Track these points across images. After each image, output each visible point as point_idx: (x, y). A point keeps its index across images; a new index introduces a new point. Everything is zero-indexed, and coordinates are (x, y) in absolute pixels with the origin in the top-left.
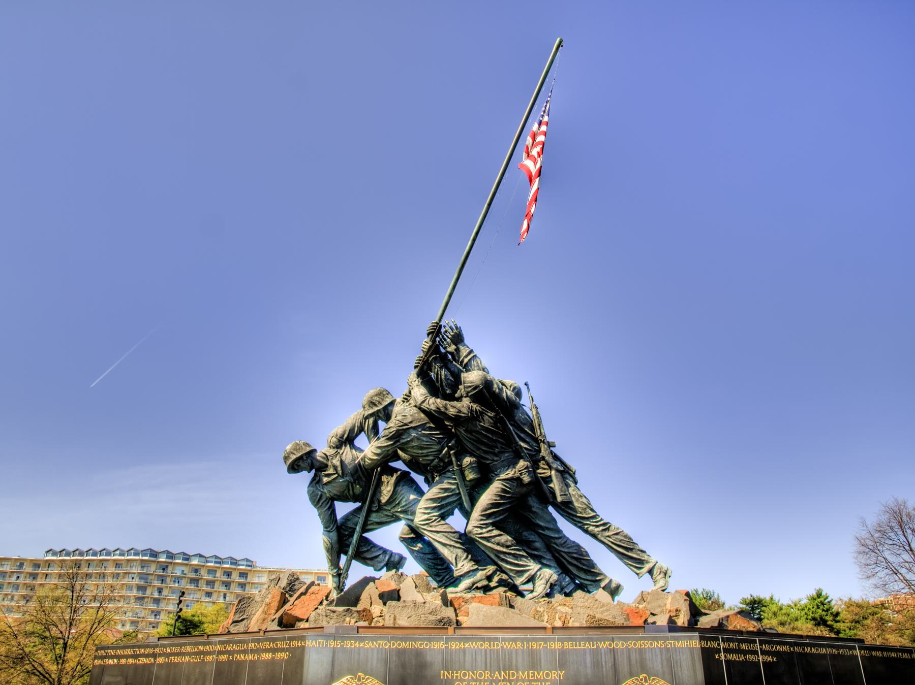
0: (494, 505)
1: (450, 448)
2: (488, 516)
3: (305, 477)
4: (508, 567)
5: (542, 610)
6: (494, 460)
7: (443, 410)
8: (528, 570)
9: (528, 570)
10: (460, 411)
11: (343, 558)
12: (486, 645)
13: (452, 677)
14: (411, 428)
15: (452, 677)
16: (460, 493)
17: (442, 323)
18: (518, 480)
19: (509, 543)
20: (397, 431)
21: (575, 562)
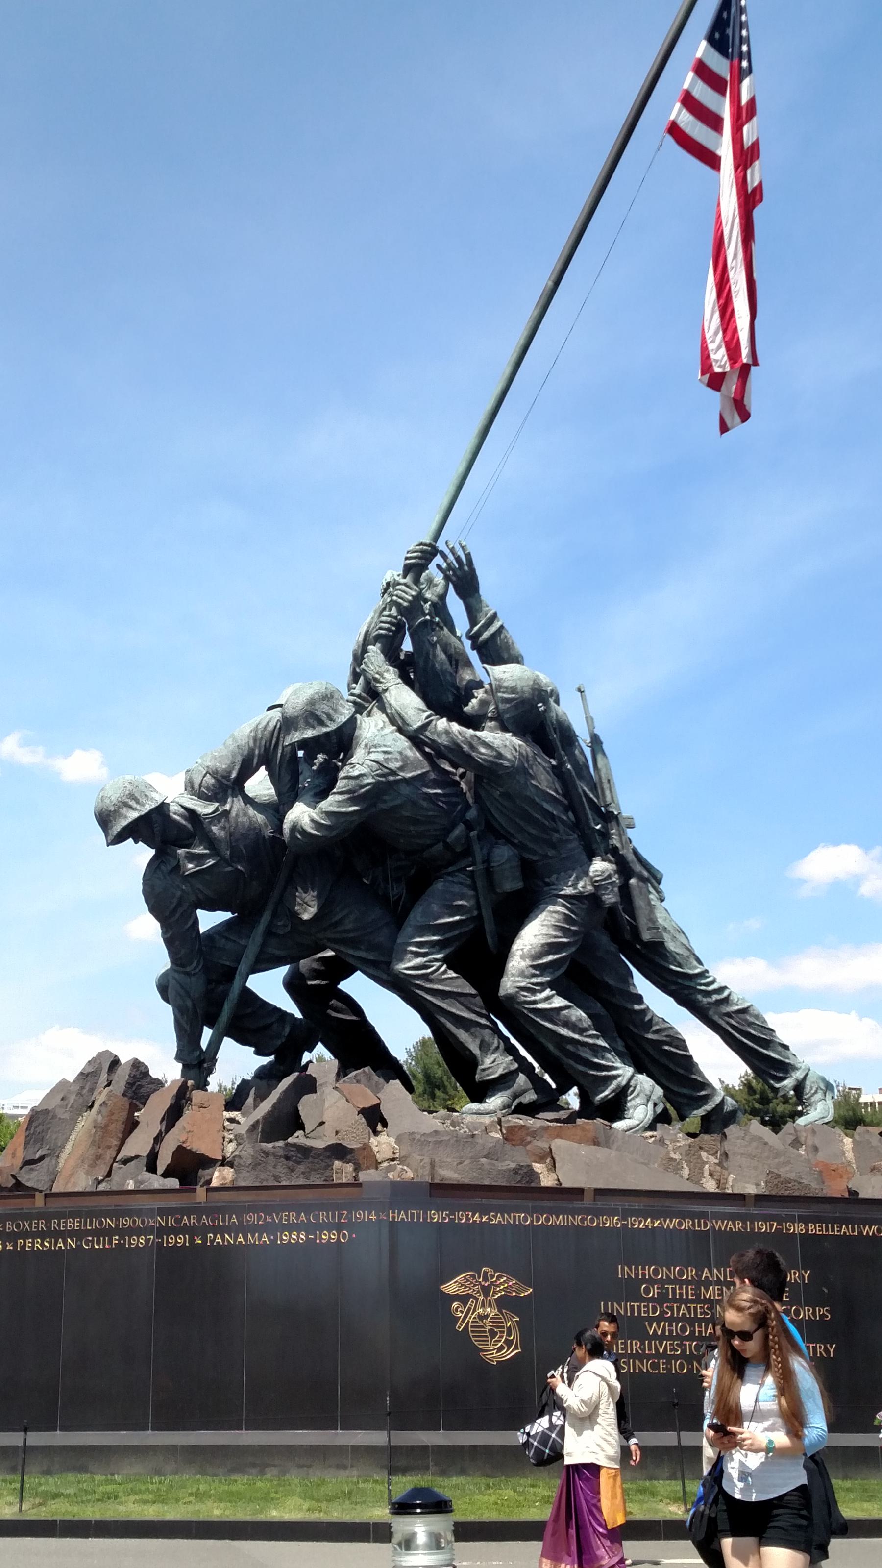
0: (551, 948)
1: (469, 826)
2: (542, 969)
3: (140, 855)
4: (581, 1068)
5: (677, 1156)
6: (546, 856)
7: (466, 748)
8: (615, 1077)
9: (615, 1077)
10: (500, 756)
11: (207, 1033)
12: (687, 1224)
13: (637, 1275)
14: (404, 780)
15: (637, 1275)
16: (480, 917)
17: (441, 545)
18: (592, 900)
19: (585, 1025)
20: (376, 785)
21: (664, 1061)
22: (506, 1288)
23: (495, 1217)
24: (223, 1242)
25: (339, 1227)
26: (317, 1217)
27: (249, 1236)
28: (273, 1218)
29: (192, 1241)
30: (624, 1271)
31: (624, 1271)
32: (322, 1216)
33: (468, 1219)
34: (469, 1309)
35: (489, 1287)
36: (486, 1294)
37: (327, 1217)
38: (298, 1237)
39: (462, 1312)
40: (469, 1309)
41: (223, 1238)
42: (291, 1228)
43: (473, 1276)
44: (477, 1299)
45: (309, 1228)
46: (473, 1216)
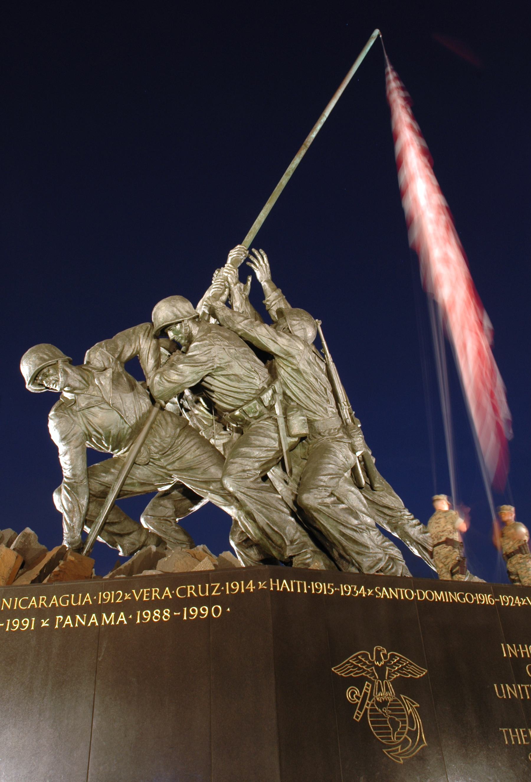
13: (519, 653)
22: (401, 669)
23: (381, 591)
24: (74, 623)
25: (209, 601)
26: (183, 592)
27: (104, 615)
28: (132, 596)
29: (38, 624)
30: (508, 650)
31: (508, 650)
32: (191, 591)
33: (353, 592)
34: (366, 694)
35: (383, 667)
36: (382, 678)
37: (196, 591)
38: (162, 614)
39: (358, 698)
40: (366, 694)
41: (74, 620)
42: (153, 605)
43: (365, 656)
44: (373, 683)
45: (176, 604)
46: (358, 589)
